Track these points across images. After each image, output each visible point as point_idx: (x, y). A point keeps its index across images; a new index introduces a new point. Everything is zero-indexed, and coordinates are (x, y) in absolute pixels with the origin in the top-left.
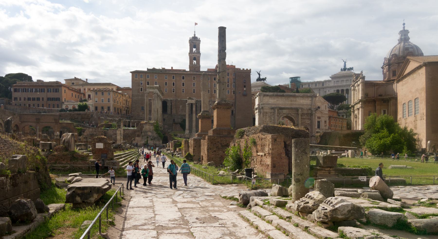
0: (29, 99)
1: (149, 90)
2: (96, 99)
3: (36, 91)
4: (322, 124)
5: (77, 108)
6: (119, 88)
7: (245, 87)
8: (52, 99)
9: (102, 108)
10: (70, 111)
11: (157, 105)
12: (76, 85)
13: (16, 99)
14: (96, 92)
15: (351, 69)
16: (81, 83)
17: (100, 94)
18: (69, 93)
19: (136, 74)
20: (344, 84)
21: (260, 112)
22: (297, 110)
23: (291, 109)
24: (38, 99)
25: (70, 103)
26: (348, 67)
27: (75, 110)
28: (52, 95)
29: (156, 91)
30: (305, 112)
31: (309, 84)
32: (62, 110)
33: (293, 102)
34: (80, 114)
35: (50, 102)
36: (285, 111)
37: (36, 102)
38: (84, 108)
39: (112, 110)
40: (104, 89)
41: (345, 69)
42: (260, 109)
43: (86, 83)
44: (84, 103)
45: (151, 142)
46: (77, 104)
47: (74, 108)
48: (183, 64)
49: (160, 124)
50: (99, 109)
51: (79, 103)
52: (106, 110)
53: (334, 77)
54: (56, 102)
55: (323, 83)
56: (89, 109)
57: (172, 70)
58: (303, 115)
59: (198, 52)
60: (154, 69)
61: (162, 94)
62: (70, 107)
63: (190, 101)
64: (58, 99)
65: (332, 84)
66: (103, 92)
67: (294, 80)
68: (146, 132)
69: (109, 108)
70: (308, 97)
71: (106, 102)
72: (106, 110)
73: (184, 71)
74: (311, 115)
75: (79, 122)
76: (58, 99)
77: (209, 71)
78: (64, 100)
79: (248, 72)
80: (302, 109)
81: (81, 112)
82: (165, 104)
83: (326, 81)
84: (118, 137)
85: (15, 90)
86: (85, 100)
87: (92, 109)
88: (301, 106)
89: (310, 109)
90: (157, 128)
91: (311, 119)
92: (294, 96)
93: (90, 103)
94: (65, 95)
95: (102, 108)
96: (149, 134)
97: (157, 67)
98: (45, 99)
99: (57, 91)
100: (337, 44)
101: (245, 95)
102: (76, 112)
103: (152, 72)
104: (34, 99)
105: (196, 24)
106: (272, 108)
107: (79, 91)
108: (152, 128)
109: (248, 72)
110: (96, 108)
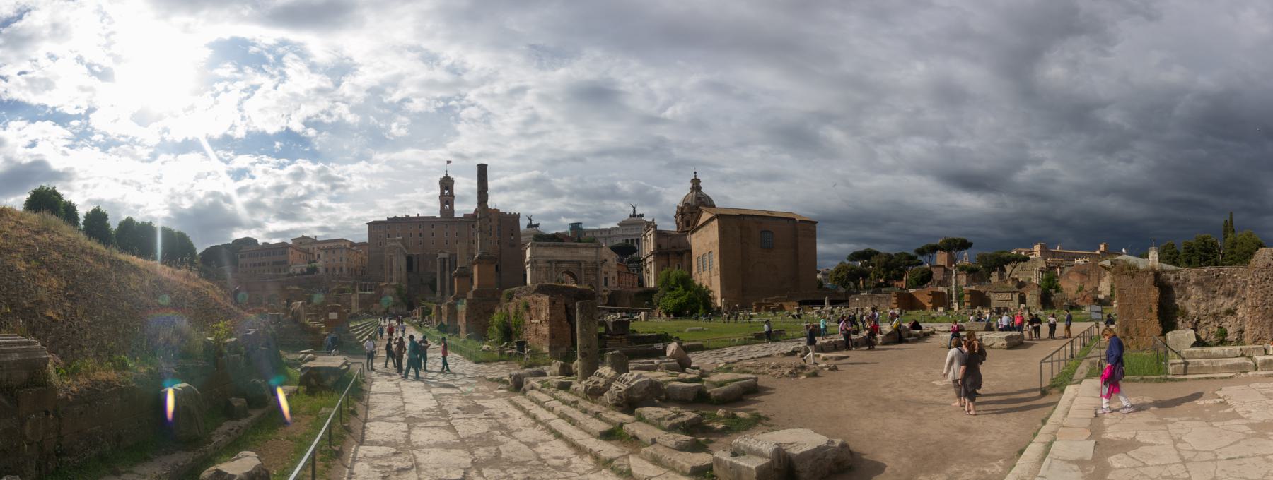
1: (389, 244)
4: (610, 281)
6: (352, 244)
11: (400, 262)
12: (304, 244)
14: (326, 250)
15: (642, 215)
19: (373, 225)
21: (532, 267)
22: (579, 263)
25: (298, 265)
26: (638, 213)
27: (302, 273)
29: (400, 244)
31: (593, 231)
32: (290, 275)
36: (564, 265)
38: (313, 270)
39: (345, 269)
40: (337, 246)
41: (634, 215)
42: (533, 262)
43: (314, 241)
45: (393, 310)
46: (305, 267)
48: (432, 208)
49: (404, 286)
50: (330, 271)
52: (337, 272)
53: (622, 224)
55: (610, 231)
58: (586, 269)
59: (452, 194)
60: (396, 218)
61: (407, 248)
62: (298, 271)
63: (441, 255)
64: (285, 263)
65: (620, 233)
66: (334, 250)
67: (575, 227)
69: (341, 269)
72: (337, 272)
74: (597, 269)
76: (285, 263)
77: (466, 216)
79: (515, 218)
82: (409, 260)
83: (613, 229)
84: (354, 304)
87: (322, 271)
90: (399, 292)
92: (576, 247)
93: (319, 264)
94: (293, 256)
97: (399, 216)
100: (624, 187)
101: (513, 246)
103: (394, 221)
105: (449, 162)
107: (307, 251)
108: (393, 291)
110: (327, 270)
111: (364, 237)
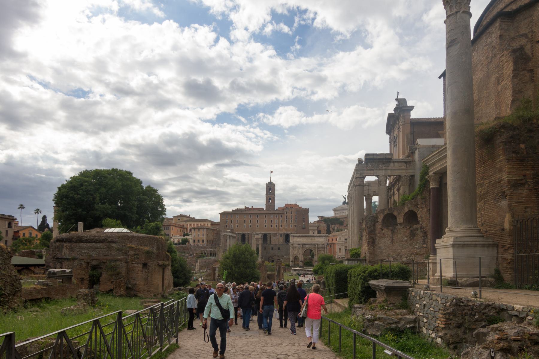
2: (194, 234)
5: (181, 242)
9: (199, 241)
10: (176, 244)
17: (197, 230)
18: (176, 229)
22: (315, 245)
23: (311, 244)
27: (179, 244)
30: (321, 246)
36: (307, 246)
38: (185, 241)
44: (186, 237)
47: (179, 241)
48: (260, 202)
50: (196, 241)
51: (182, 237)
52: (201, 242)
56: (189, 242)
57: (253, 209)
59: (273, 194)
62: (176, 241)
69: (203, 241)
71: (201, 236)
72: (201, 242)
75: (181, 252)
76: (168, 235)
79: (306, 211)
80: (318, 244)
81: (184, 245)
86: (188, 235)
87: (191, 242)
91: (324, 251)
95: (199, 241)
102: (181, 245)
105: (272, 172)
106: (299, 244)
109: (306, 211)
110: (194, 241)
111: (217, 219)
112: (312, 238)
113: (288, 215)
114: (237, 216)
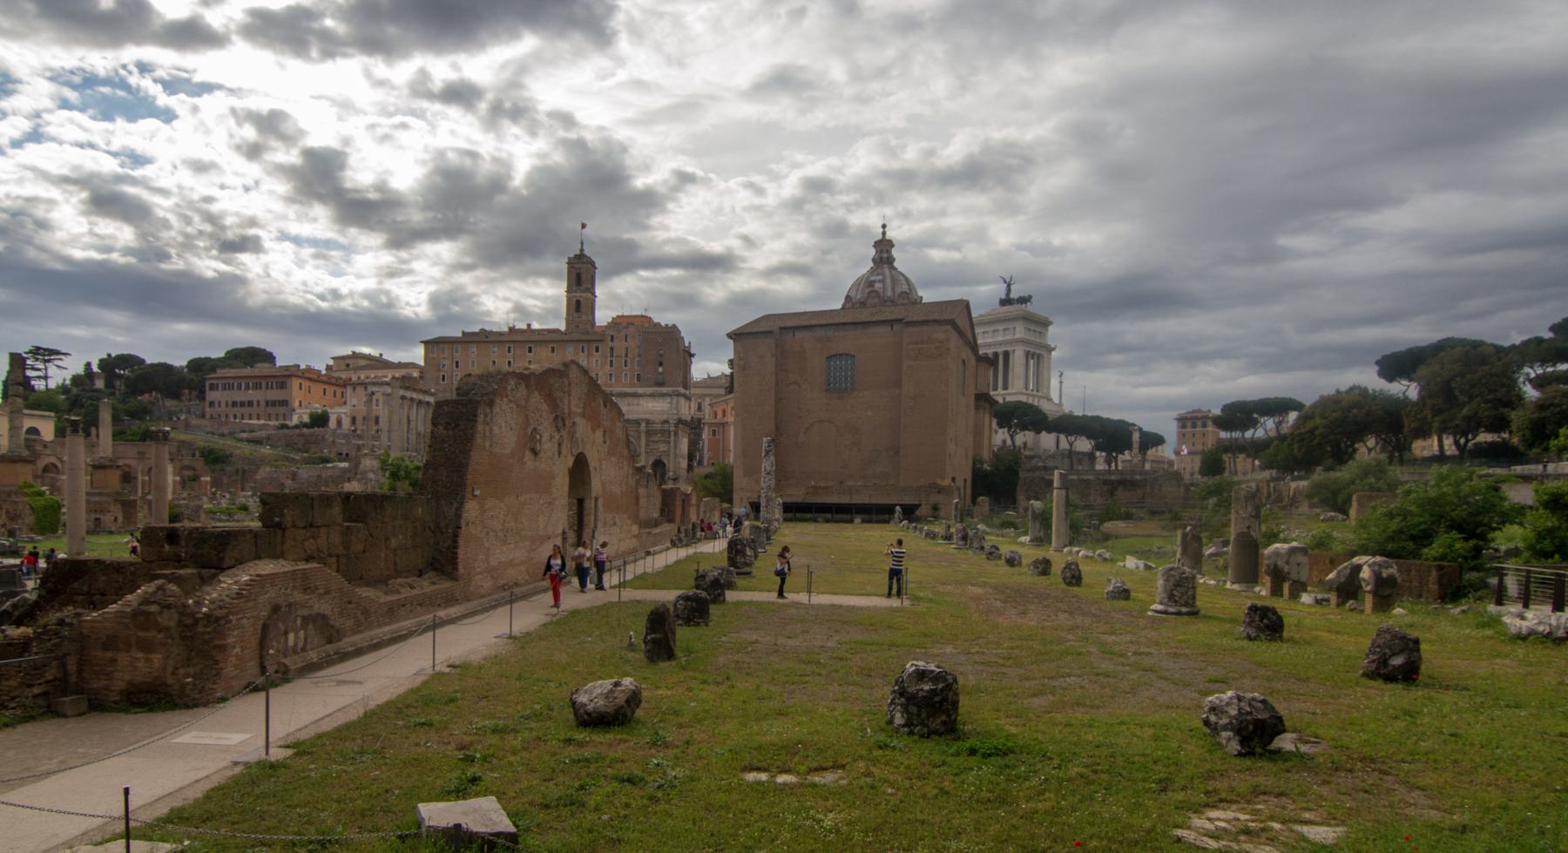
0: (234, 404)
2: (354, 402)
3: (247, 388)
7: (661, 364)
8: (274, 403)
13: (212, 404)
16: (363, 362)
20: (1000, 338)
24: (250, 404)
28: (274, 395)
30: (658, 427)
33: (635, 408)
34: (302, 435)
35: (271, 410)
37: (246, 410)
41: (1006, 302)
50: (359, 421)
54: (282, 409)
64: (284, 403)
68: (365, 472)
70: (663, 395)
73: (556, 331)
76: (284, 403)
78: (297, 404)
80: (648, 422)
85: (212, 387)
88: (648, 416)
89: (666, 422)
96: (371, 476)
98: (263, 403)
99: (283, 386)
104: (242, 404)
108: (376, 464)
110: (354, 420)
112: (631, 400)
113: (616, 344)
114: (474, 349)
